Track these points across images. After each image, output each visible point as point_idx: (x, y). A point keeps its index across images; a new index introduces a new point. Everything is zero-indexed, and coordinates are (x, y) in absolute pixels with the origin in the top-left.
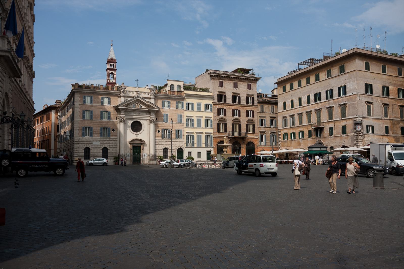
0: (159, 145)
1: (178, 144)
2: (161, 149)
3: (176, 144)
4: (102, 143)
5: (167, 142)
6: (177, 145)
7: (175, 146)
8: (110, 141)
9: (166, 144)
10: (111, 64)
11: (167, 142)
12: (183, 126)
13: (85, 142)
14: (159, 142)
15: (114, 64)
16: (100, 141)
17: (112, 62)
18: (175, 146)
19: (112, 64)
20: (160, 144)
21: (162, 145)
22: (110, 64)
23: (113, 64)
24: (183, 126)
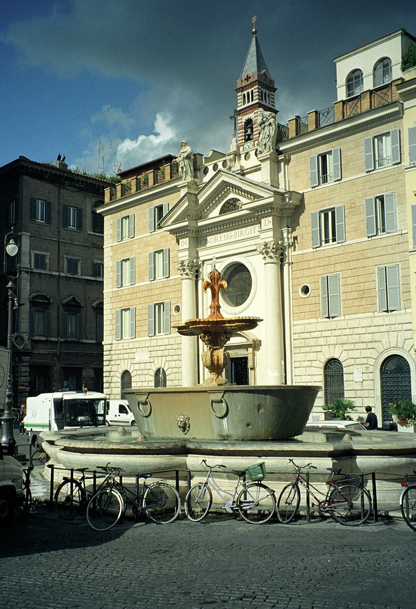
0: (308, 349)
1: (384, 338)
2: (315, 364)
3: (377, 337)
4: (154, 354)
5: (337, 333)
6: (376, 345)
7: (370, 345)
8: (169, 347)
9: (332, 340)
10: (245, 92)
11: (337, 333)
12: (401, 248)
13: (121, 357)
14: (308, 335)
15: (252, 91)
16: (150, 349)
17: (246, 86)
18: (370, 345)
19: (248, 93)
20: (312, 342)
21: (318, 349)
22: (244, 95)
23: (249, 91)
24: (401, 248)
